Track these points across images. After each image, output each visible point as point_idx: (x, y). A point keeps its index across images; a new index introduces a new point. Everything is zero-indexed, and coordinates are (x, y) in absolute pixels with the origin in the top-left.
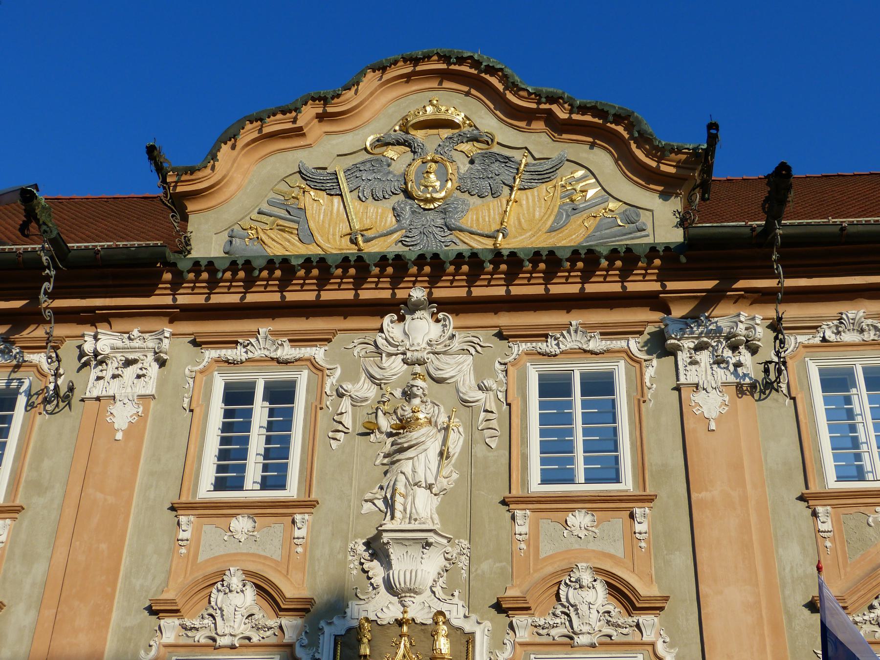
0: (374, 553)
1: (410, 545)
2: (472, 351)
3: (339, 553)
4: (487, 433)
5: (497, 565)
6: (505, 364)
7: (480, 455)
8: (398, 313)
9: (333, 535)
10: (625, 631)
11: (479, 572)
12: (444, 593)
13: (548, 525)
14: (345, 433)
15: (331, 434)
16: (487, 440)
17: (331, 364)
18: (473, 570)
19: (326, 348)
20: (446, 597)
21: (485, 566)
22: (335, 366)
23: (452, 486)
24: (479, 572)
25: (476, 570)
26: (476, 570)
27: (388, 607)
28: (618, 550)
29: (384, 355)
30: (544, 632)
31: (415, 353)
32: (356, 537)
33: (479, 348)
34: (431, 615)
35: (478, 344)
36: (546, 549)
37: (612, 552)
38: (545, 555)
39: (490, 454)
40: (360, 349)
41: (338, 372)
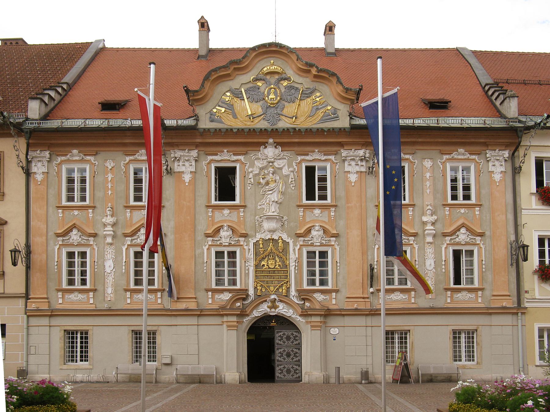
4: (291, 186)
5: (295, 224)
10: (327, 242)
13: (308, 212)
20: (282, 233)
21: (292, 224)
28: (326, 220)
30: (307, 242)
36: (308, 220)
37: (325, 220)
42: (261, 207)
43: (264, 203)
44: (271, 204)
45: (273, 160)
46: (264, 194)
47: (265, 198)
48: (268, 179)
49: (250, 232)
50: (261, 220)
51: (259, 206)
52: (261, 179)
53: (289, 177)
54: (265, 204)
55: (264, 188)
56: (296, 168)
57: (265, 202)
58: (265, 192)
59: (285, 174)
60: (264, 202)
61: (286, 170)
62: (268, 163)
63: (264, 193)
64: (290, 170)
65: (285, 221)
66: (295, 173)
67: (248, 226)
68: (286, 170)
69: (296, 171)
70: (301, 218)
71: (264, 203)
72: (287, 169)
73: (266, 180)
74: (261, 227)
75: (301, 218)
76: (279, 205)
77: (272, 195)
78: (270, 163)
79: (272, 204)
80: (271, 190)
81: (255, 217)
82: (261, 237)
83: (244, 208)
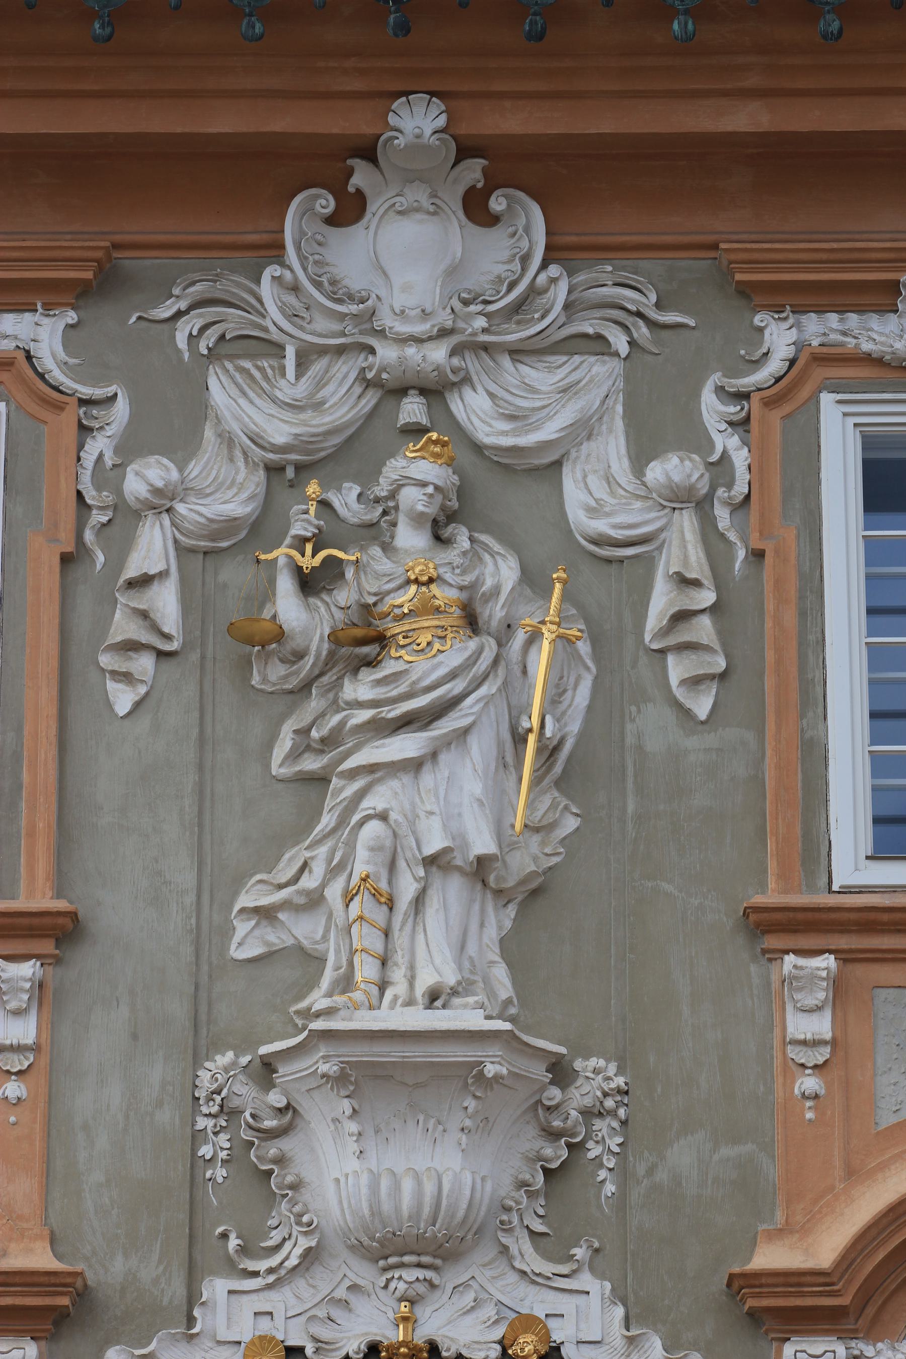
0: (288, 1106)
1: (417, 1086)
2: (620, 342)
3: (160, 1104)
5: (726, 1151)
6: (742, 396)
7: (654, 744)
8: (338, 189)
9: (135, 1037)
11: (662, 1176)
12: (537, 1249)
14: (161, 655)
15: (106, 660)
16: (679, 693)
17: (95, 382)
18: (641, 1170)
19: (71, 317)
20: (548, 1268)
22: (110, 391)
23: (555, 860)
24: (662, 1176)
25: (651, 1171)
26: (651, 1171)
27: (345, 1304)
29: (290, 351)
31: (411, 351)
32: (217, 1047)
33: (642, 331)
34: (499, 1332)
35: (639, 314)
38: (893, 1120)
39: (692, 742)
40: (199, 323)
41: (121, 410)
42: (275, 938)
43: (309, 882)
44: (407, 888)
45: (438, 354)
46: (320, 780)
47: (327, 820)
48: (371, 585)
49: (118, 1266)
50: (276, 1099)
51: (242, 927)
52: (285, 584)
53: (648, 563)
54: (334, 892)
55: (315, 704)
56: (740, 458)
57: (333, 872)
58: (329, 742)
59: (601, 526)
60: (319, 869)
61: (609, 480)
62: (371, 399)
63: (311, 764)
64: (655, 472)
65: (588, 1114)
66: (722, 516)
67: (98, 1176)
68: (609, 480)
69: (741, 488)
70: (810, 1083)
71: (309, 882)
72: (621, 467)
73: (344, 596)
74: (271, 1199)
75: (810, 1083)
76: (511, 911)
77: (427, 778)
78: (402, 392)
79: (419, 901)
80: (406, 723)
81: (197, 1063)
82: (265, 1326)
83: (48, 947)
